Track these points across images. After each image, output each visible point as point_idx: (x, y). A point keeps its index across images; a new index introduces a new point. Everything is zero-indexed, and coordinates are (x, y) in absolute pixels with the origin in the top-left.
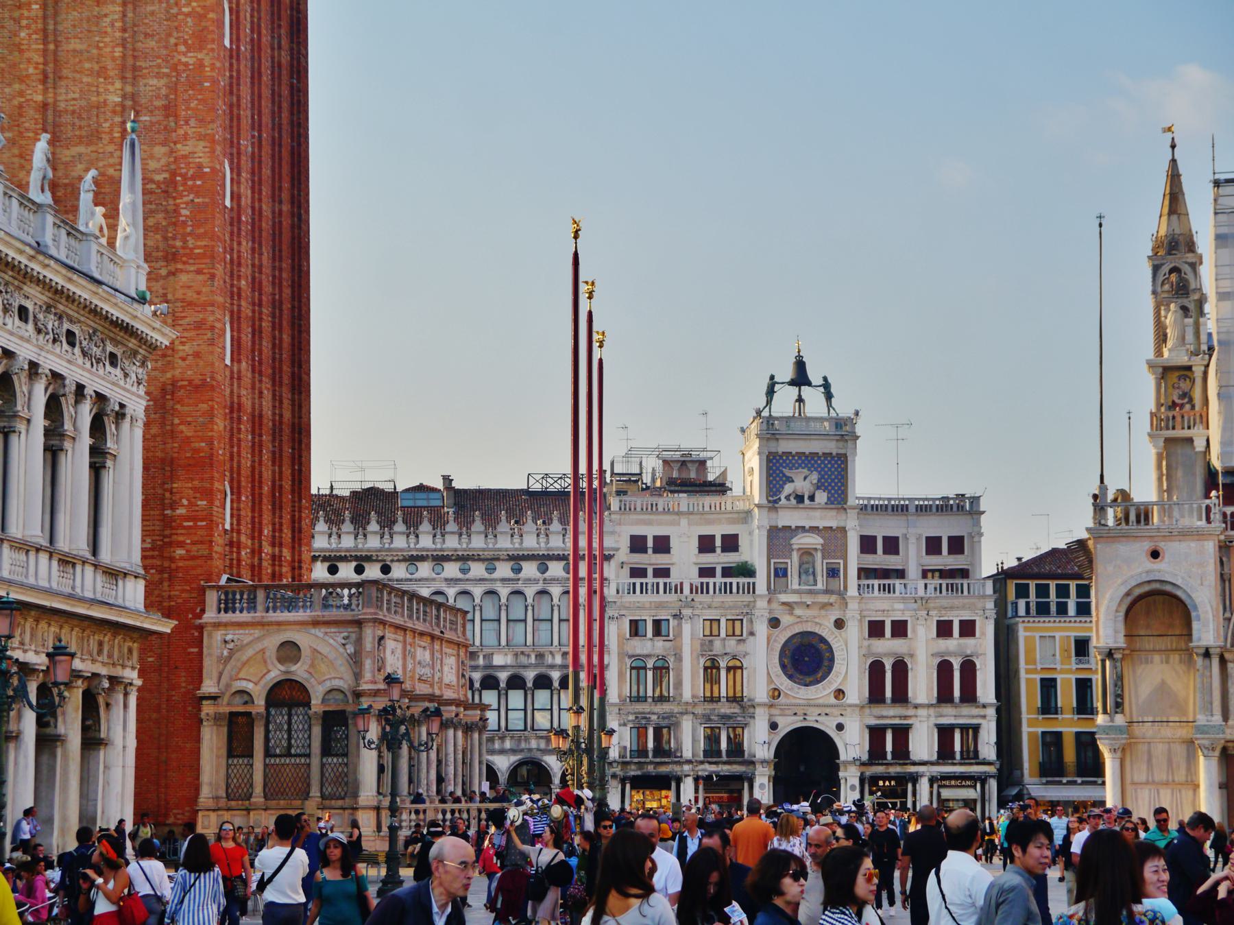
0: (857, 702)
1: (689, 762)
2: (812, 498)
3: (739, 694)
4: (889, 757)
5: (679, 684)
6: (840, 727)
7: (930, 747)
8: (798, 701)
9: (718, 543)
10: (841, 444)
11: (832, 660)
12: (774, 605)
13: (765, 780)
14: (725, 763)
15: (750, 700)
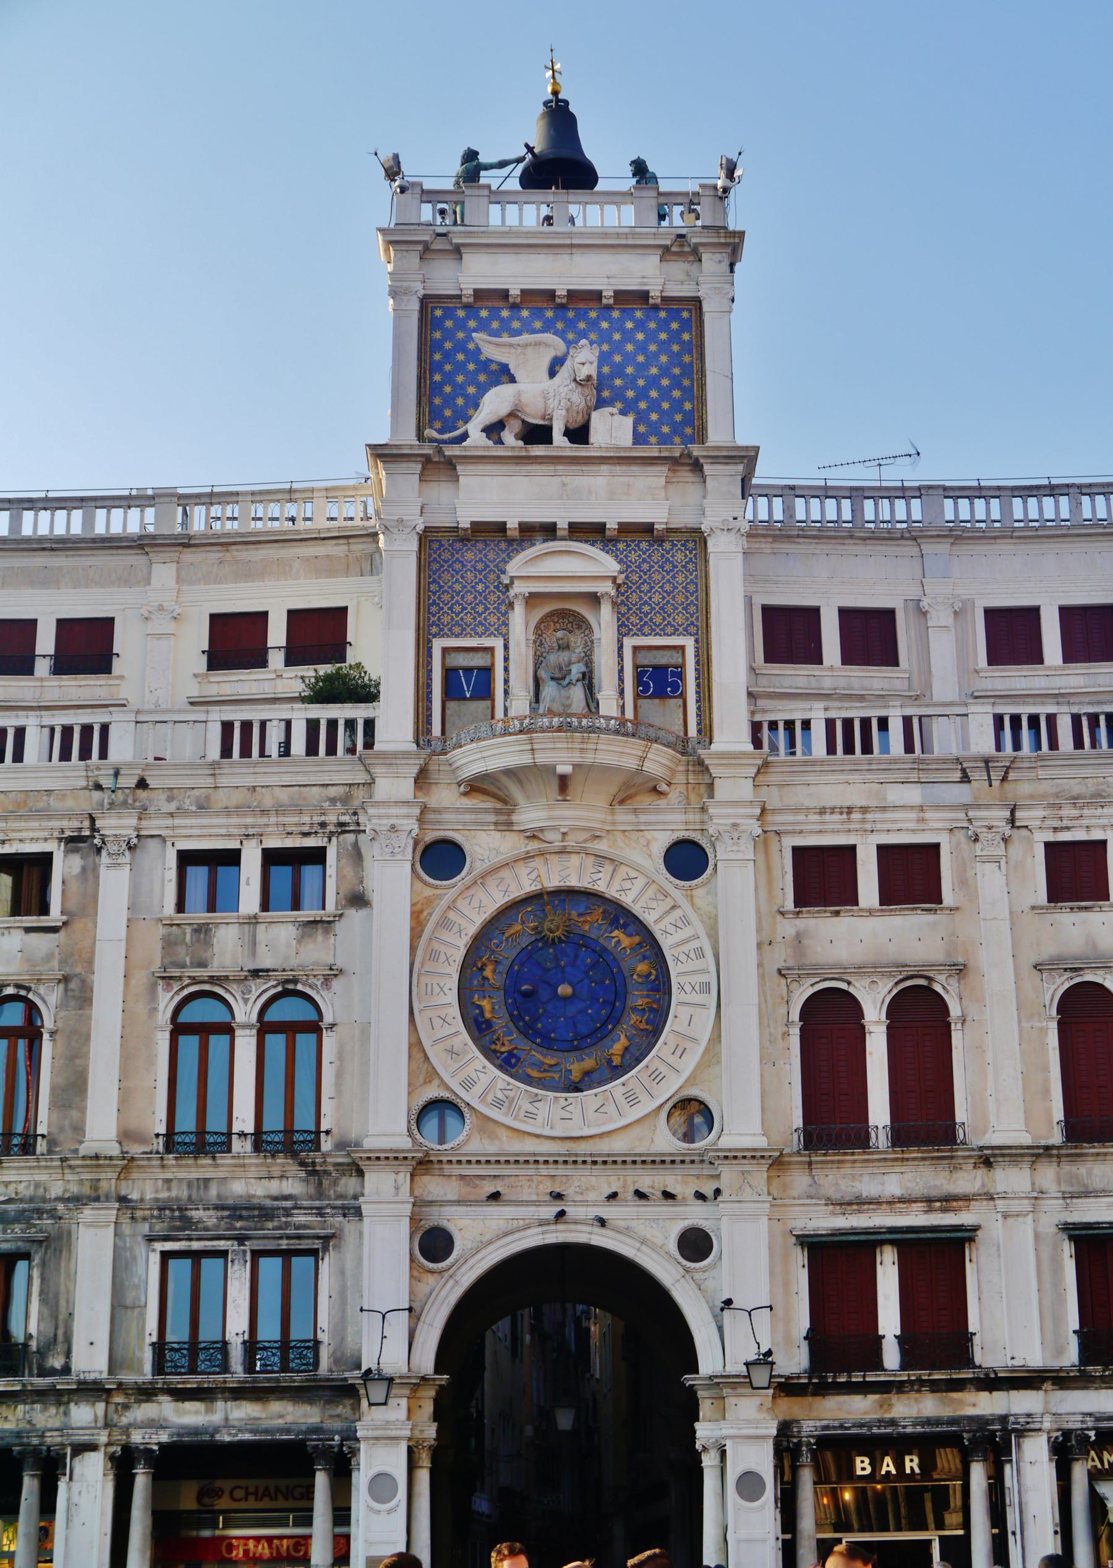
0: (761, 1142)
1: (92, 1390)
2: (579, 434)
3: (303, 1121)
4: (891, 1357)
5: (74, 1089)
6: (695, 1245)
7: (1051, 1316)
8: (530, 1146)
9: (277, 634)
10: (677, 268)
11: (660, 984)
12: (445, 796)
13: (395, 1462)
14: (238, 1394)
15: (341, 1145)
